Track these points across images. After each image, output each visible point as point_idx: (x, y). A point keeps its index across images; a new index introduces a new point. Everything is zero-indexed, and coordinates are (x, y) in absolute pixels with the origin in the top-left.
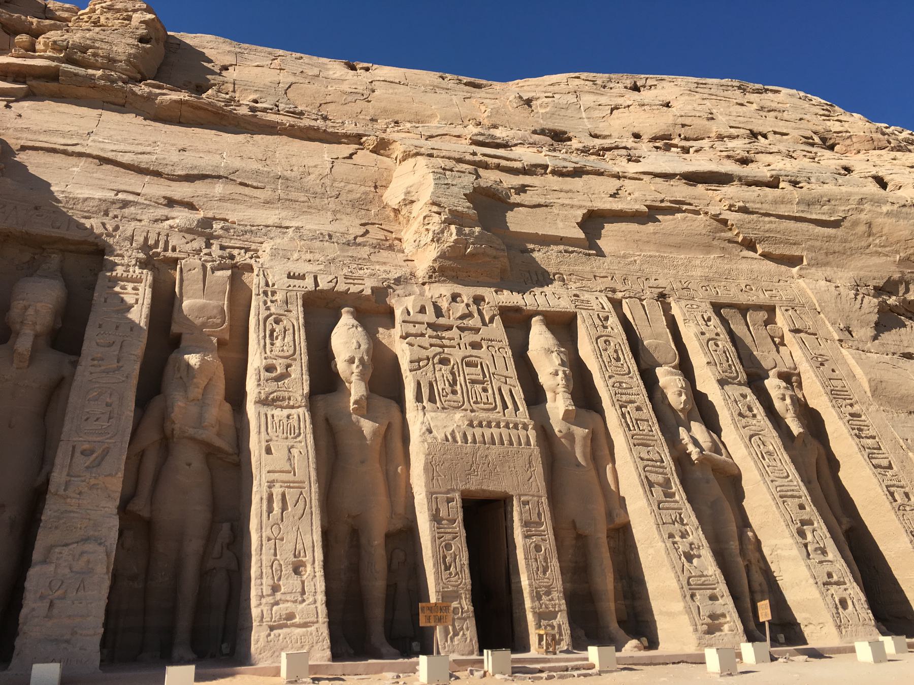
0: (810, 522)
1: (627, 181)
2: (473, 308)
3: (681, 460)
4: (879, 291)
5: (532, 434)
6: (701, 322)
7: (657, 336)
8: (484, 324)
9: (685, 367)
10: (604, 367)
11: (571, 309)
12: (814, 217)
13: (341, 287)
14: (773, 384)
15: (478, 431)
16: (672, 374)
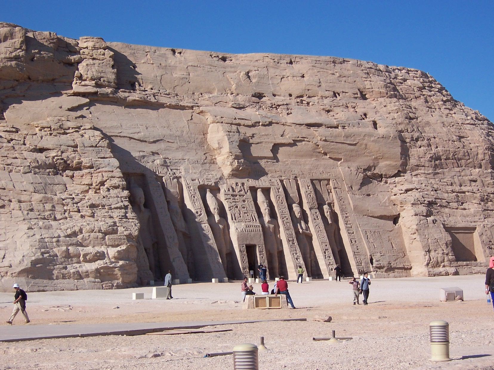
0: (328, 250)
1: (287, 127)
2: (242, 187)
3: (297, 232)
4: (365, 170)
5: (261, 228)
6: (307, 187)
7: (293, 193)
8: (246, 193)
9: (301, 204)
10: (278, 206)
11: (269, 186)
12: (348, 142)
13: (206, 183)
14: (326, 208)
15: (248, 228)
16: (297, 207)
